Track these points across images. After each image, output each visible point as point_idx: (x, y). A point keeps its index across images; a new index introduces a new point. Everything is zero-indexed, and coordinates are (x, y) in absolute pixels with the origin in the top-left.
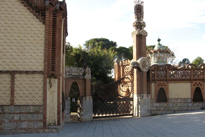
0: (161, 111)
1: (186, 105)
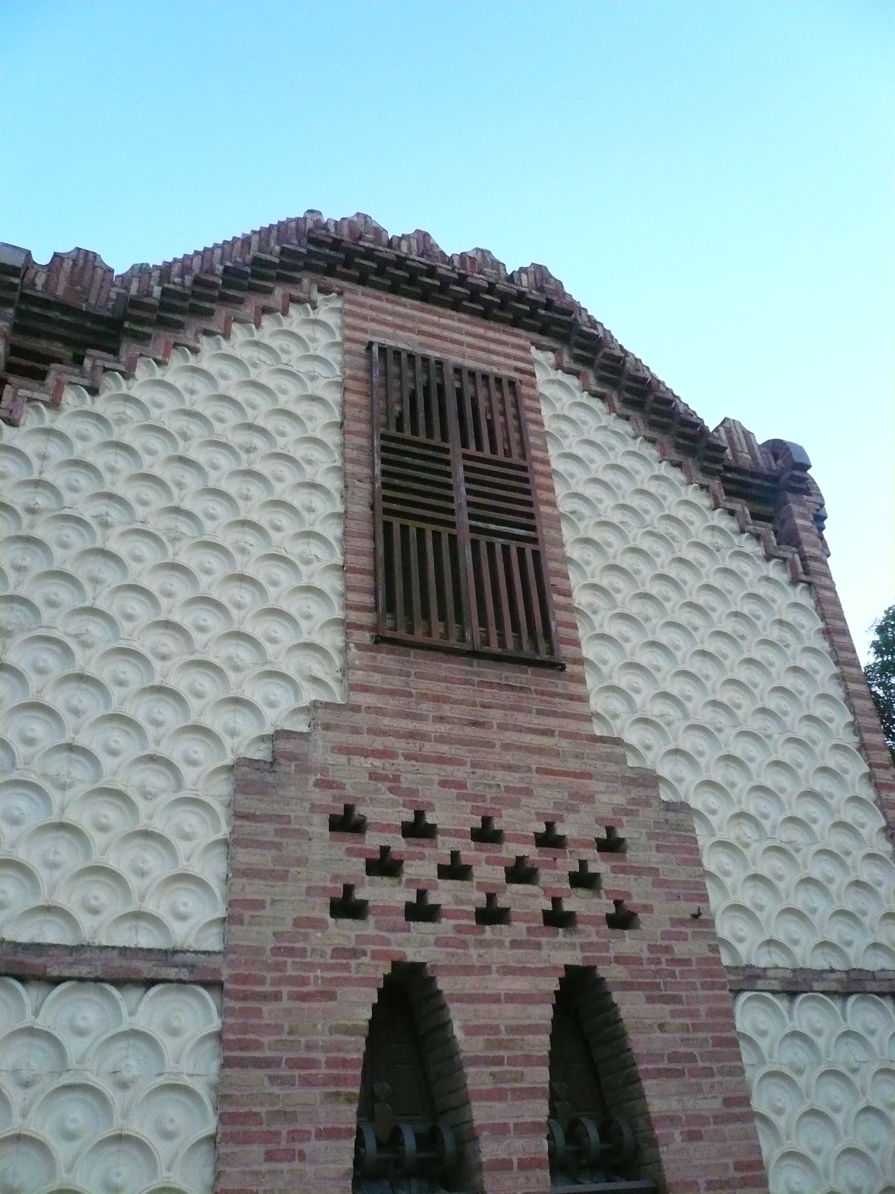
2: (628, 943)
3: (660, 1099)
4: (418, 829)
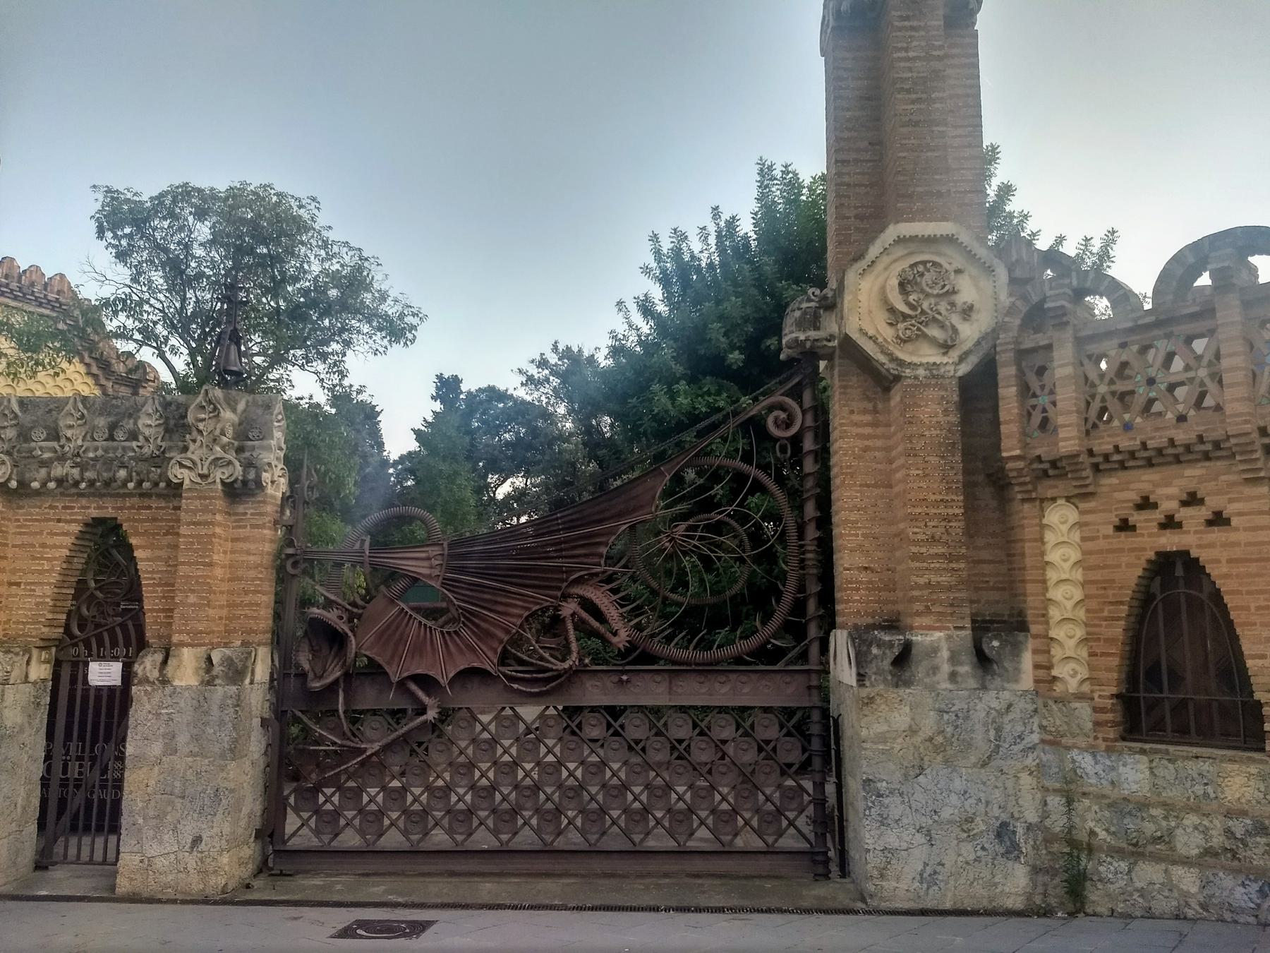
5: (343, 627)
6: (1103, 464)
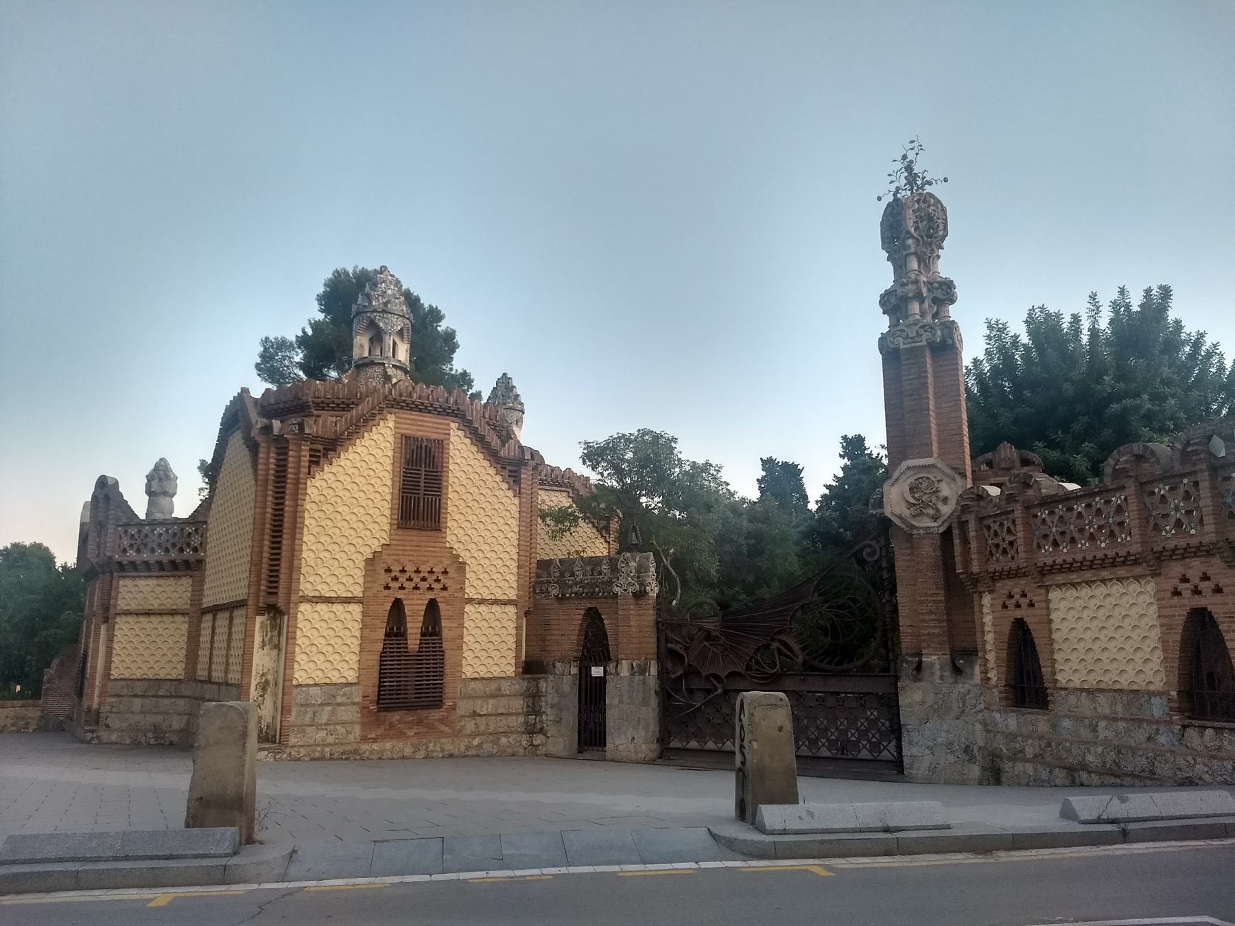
0: (1029, 761)
1: (1140, 736)
2: (445, 593)
3: (444, 623)
4: (403, 571)
5: (682, 652)
6: (997, 577)
